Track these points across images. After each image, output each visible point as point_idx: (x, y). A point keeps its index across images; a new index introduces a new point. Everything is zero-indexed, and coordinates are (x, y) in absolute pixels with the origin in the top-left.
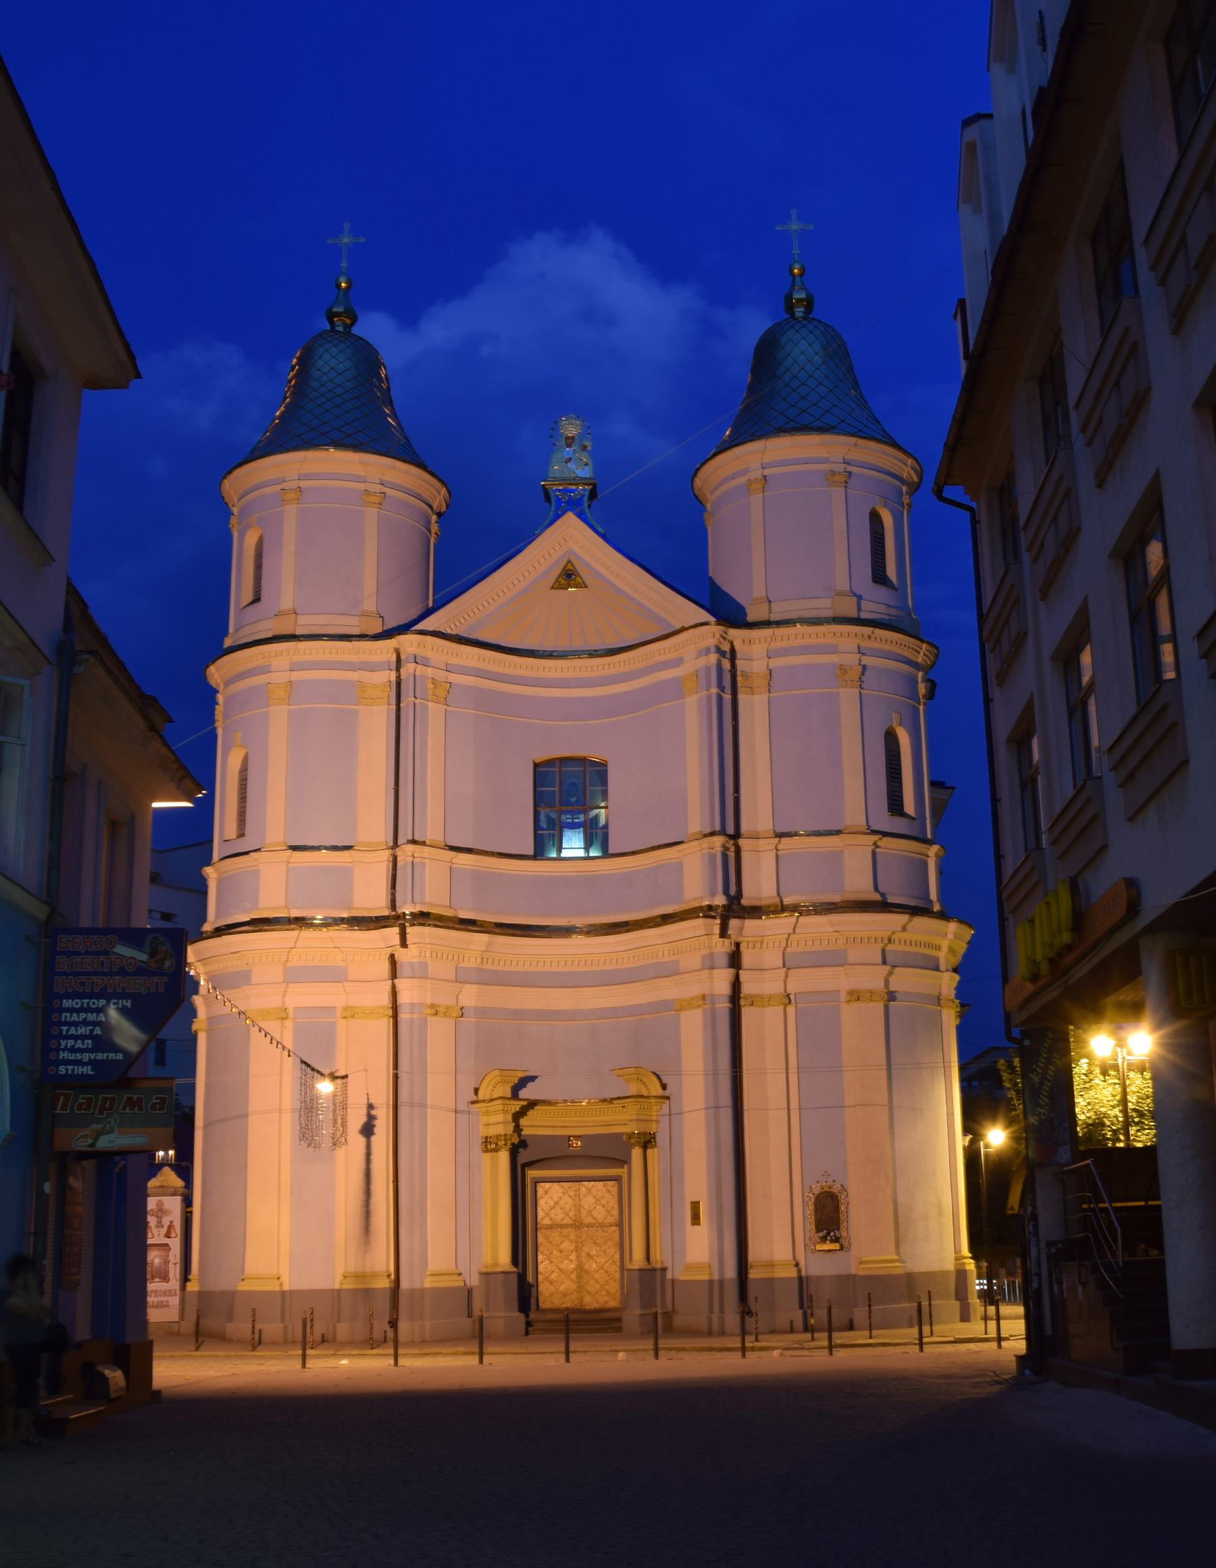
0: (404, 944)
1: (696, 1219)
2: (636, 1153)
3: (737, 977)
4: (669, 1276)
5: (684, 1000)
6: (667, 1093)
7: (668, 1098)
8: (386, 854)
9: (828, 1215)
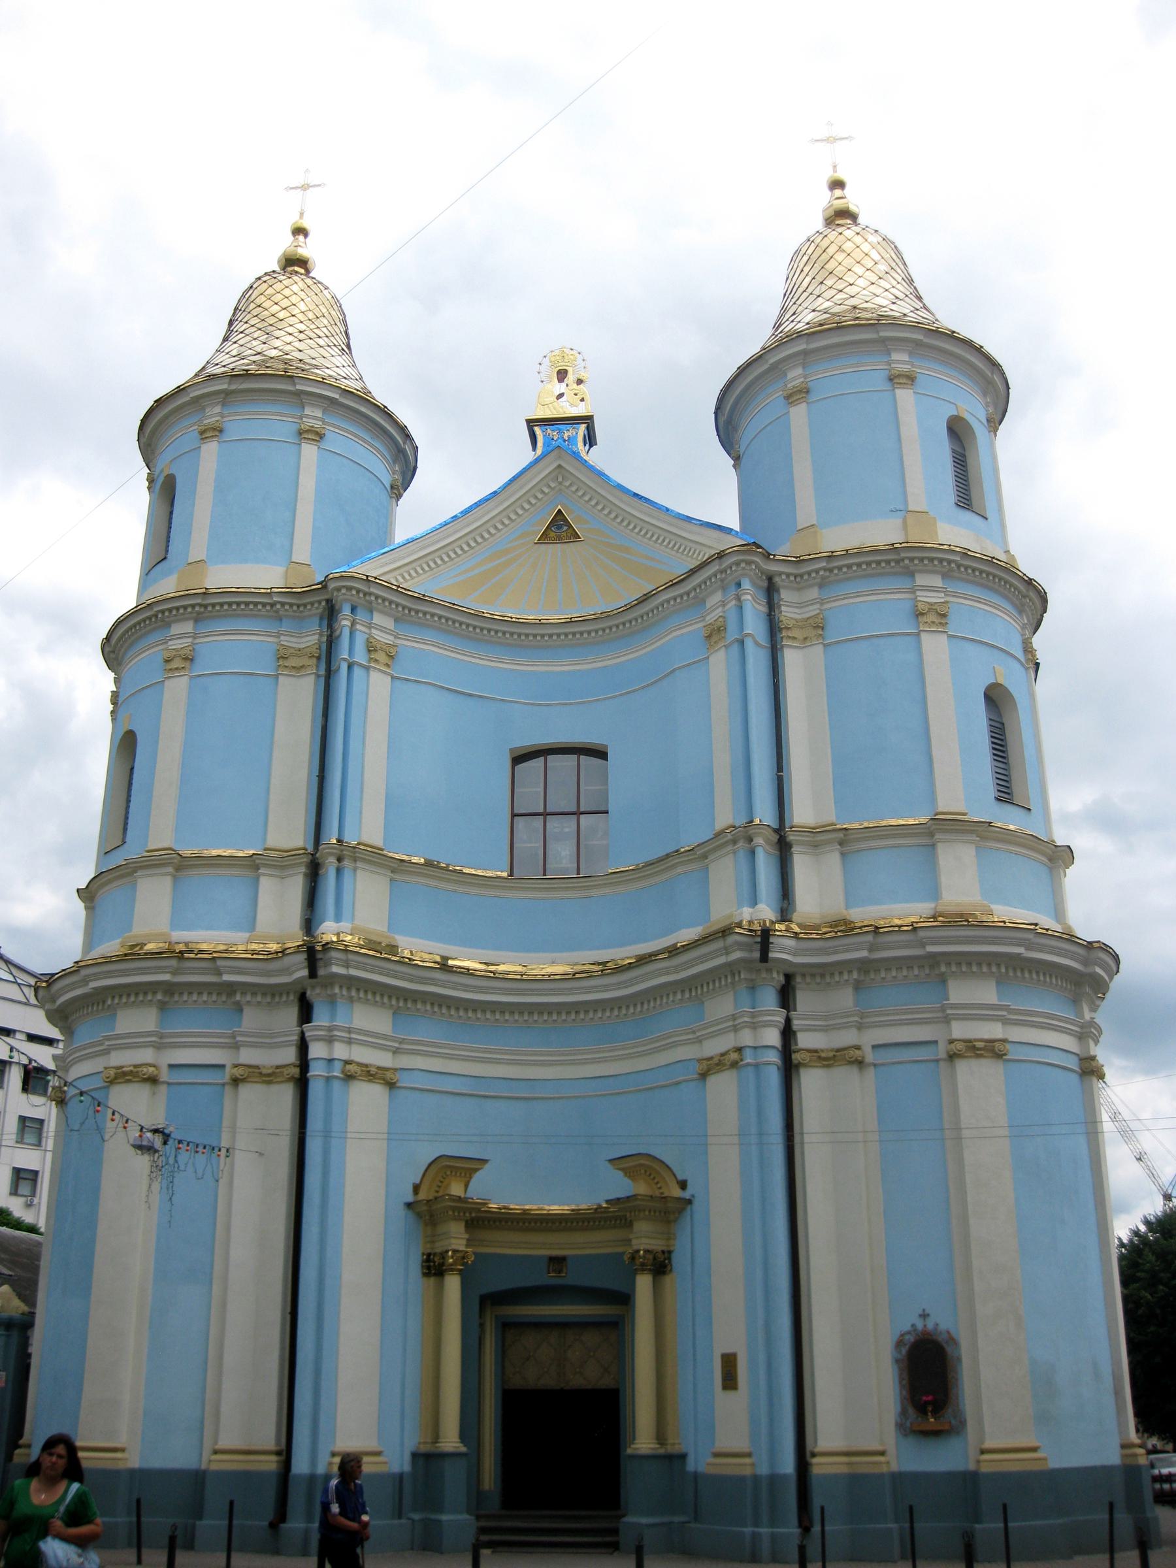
0: (313, 974)
1: (730, 1380)
2: (643, 1284)
3: (788, 1021)
4: (691, 1466)
5: (711, 1058)
6: (686, 1195)
7: (689, 1202)
8: (306, 859)
9: (929, 1374)
